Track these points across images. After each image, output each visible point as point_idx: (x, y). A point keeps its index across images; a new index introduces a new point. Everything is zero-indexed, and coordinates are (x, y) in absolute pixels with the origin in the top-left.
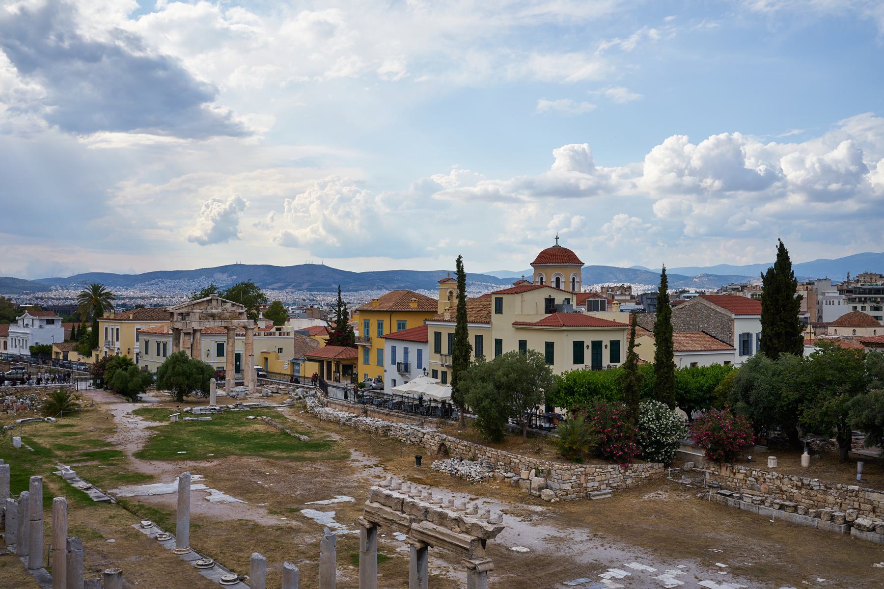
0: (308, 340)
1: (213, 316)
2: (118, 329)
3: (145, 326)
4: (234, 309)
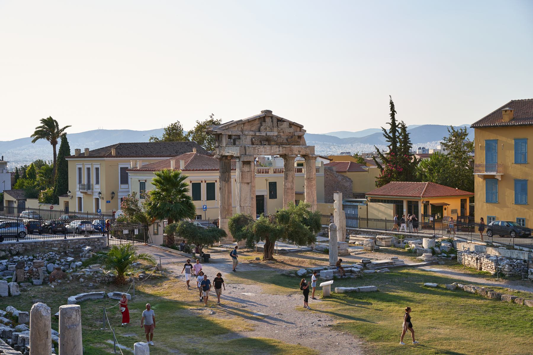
0: (340, 178)
1: (267, 141)
2: (97, 169)
3: (131, 163)
4: (292, 130)
